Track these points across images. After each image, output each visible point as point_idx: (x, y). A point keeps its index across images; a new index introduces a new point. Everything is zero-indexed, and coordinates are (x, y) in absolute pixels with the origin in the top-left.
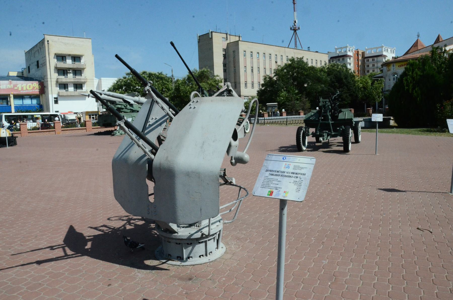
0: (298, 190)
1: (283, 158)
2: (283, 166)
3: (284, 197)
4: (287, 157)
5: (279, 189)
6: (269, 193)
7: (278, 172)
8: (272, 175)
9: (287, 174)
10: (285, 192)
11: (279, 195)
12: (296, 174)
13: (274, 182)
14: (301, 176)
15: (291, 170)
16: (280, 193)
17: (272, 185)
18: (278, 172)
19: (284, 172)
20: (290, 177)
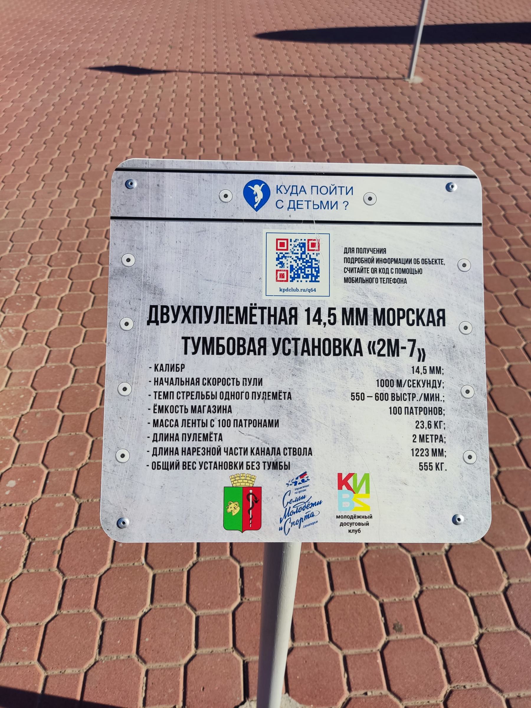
0: (430, 454)
1: (249, 195)
3: (353, 521)
4: (273, 182)
5: (299, 465)
6: (236, 509)
7: (244, 315)
8: (209, 346)
9: (316, 332)
10: (343, 482)
11: (301, 509)
12: (381, 317)
13: (241, 409)
14: (424, 334)
15: (333, 291)
16: (312, 492)
17: (232, 437)
18: (244, 315)
19: (288, 316)
20: (340, 348)
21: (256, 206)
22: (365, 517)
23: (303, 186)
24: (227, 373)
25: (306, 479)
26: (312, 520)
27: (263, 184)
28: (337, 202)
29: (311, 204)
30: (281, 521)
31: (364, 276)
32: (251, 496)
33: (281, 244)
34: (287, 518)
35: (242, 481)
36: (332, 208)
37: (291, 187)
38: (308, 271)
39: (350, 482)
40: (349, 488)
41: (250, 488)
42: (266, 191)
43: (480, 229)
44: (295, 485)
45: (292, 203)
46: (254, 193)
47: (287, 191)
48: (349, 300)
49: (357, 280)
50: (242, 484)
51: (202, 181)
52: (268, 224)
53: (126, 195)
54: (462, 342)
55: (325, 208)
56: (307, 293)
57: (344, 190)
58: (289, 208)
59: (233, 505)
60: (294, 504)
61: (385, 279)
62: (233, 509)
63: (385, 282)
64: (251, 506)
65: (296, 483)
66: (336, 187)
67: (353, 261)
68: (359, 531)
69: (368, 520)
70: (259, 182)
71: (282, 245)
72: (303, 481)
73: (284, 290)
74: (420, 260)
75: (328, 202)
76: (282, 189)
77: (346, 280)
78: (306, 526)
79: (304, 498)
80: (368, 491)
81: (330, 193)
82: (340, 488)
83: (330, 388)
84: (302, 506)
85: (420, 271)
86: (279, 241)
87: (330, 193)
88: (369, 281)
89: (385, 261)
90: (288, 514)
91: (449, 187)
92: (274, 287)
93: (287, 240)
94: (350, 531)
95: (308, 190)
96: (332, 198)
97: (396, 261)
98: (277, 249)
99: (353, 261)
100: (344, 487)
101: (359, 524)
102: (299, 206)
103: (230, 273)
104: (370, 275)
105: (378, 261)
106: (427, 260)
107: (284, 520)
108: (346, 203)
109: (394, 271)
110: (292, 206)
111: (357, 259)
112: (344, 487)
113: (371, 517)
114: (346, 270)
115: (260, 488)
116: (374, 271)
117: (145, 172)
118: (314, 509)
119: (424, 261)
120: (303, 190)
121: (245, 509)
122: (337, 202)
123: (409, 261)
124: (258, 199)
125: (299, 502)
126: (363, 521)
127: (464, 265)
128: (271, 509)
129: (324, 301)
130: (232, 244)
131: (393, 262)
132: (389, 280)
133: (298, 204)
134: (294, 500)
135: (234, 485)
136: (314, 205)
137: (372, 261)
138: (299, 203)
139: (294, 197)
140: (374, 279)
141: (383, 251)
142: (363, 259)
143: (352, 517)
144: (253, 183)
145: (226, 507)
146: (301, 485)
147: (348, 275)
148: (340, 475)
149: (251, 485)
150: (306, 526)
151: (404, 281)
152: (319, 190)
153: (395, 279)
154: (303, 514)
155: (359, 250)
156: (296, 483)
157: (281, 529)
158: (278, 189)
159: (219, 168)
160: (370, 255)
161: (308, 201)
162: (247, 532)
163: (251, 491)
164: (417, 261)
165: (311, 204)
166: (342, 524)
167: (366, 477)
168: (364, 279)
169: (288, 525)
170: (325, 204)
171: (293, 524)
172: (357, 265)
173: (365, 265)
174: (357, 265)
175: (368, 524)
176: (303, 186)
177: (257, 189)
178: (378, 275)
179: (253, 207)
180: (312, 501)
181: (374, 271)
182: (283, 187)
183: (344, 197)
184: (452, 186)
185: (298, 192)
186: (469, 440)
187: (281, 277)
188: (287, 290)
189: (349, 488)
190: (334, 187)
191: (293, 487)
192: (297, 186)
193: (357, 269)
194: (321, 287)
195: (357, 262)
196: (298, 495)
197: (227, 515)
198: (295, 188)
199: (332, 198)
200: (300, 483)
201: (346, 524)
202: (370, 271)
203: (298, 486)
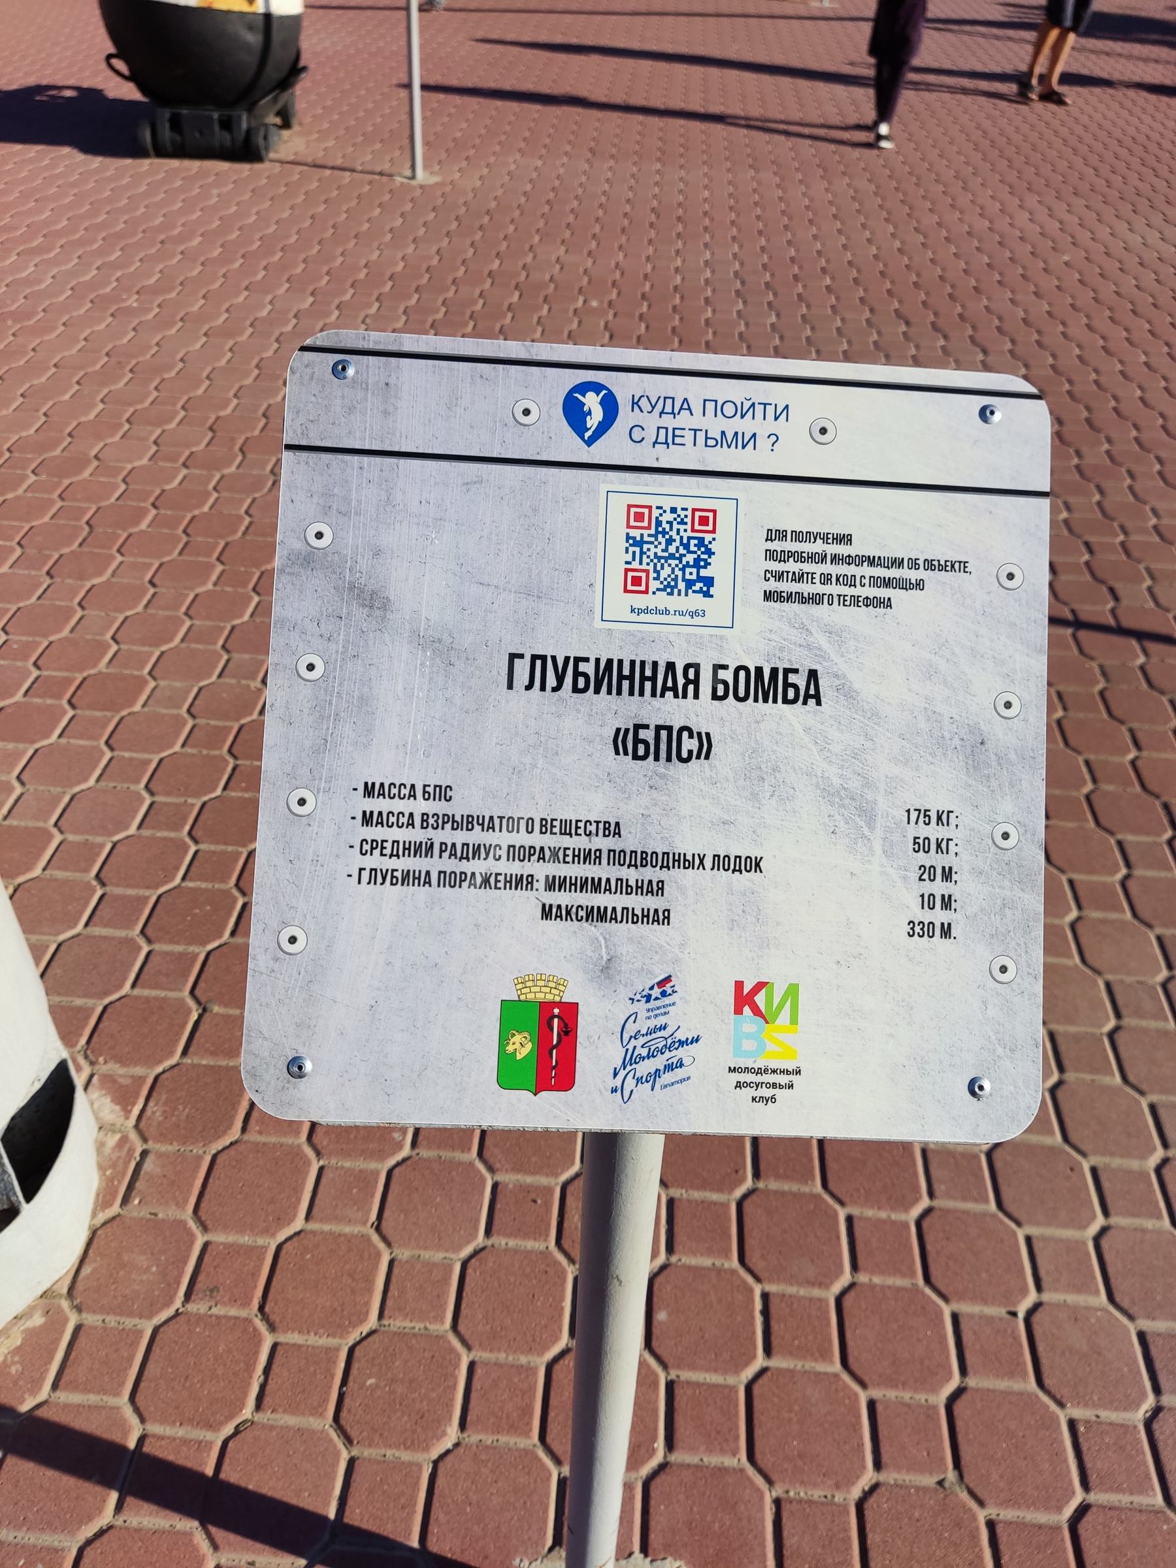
1: (574, 412)
2: (619, 557)
3: (763, 1081)
6: (523, 1047)
11: (656, 1054)
16: (682, 1017)
21: (587, 435)
22: (788, 1072)
23: (685, 399)
24: (514, 776)
25: (669, 991)
26: (679, 1073)
27: (604, 392)
28: (754, 435)
29: (701, 436)
30: (615, 1075)
31: (806, 588)
32: (556, 1020)
33: (637, 514)
34: (629, 1068)
35: (538, 989)
36: (744, 447)
37: (662, 400)
38: (691, 574)
39: (760, 999)
40: (757, 1011)
41: (554, 1004)
42: (610, 406)
43: (1046, 503)
44: (648, 1001)
45: (662, 432)
46: (586, 408)
47: (653, 408)
48: (773, 636)
49: (790, 597)
50: (538, 995)
51: (479, 380)
52: (611, 475)
53: (320, 400)
54: (999, 733)
55: (729, 447)
56: (687, 620)
57: (770, 410)
58: (655, 443)
59: (518, 1038)
60: (642, 1040)
61: (848, 598)
62: (518, 1046)
63: (847, 603)
64: (555, 1042)
65: (648, 998)
66: (753, 404)
67: (785, 556)
68: (773, 1099)
69: (791, 1077)
70: (596, 387)
71: (639, 517)
72: (664, 994)
73: (640, 612)
74: (921, 562)
75: (736, 434)
76: (644, 403)
77: (768, 596)
78: (666, 1086)
79: (665, 1028)
80: (794, 1020)
81: (742, 416)
82: (738, 1011)
83: (727, 818)
84: (660, 1045)
85: (919, 585)
86: (633, 510)
87: (742, 416)
88: (816, 599)
89: (849, 560)
90: (631, 1060)
91: (985, 414)
92: (619, 603)
93: (650, 508)
94: (754, 1099)
95: (697, 408)
96: (746, 426)
97: (872, 561)
98: (628, 526)
99: (785, 556)
100: (747, 1010)
101: (774, 1085)
102: (677, 440)
103: (530, 570)
104: (818, 588)
105: (836, 559)
106: (936, 563)
107: (622, 1073)
108: (773, 438)
109: (866, 581)
110: (662, 439)
111: (791, 554)
112: (747, 1010)
113: (798, 1072)
114: (768, 575)
115: (575, 1006)
116: (826, 579)
117: (360, 357)
118: (681, 1053)
119: (930, 565)
120: (685, 406)
121: (543, 1047)
122: (754, 435)
123: (898, 563)
124: (593, 422)
125: (654, 1036)
126: (783, 1079)
127: (1011, 576)
128: (596, 1053)
129: (722, 638)
130: (535, 510)
131: (865, 564)
132: (855, 601)
133: (674, 436)
134: (644, 1031)
135: (523, 997)
136: (707, 438)
137: (823, 559)
138: (677, 432)
139: (667, 421)
140: (826, 597)
141: (845, 539)
142: (805, 555)
143: (759, 1072)
144: (584, 388)
145: (503, 1041)
146: (658, 1003)
147: (773, 585)
148: (739, 985)
149: (557, 999)
150: (666, 1086)
151: (887, 603)
152: (719, 409)
153: (867, 598)
154: (659, 1062)
155: (798, 536)
156: (648, 998)
157: (614, 1090)
158: (635, 403)
159: (513, 355)
160: (818, 547)
161: (695, 430)
162: (543, 1093)
163: (556, 1011)
164: (914, 564)
165: (701, 436)
166: (739, 1085)
167: (793, 991)
168: (806, 595)
169: (630, 1083)
170: (730, 437)
171: (639, 1081)
172: (792, 566)
173: (807, 567)
174: (792, 566)
175: (791, 1086)
176: (685, 399)
177: (592, 401)
178: (834, 589)
179: (582, 438)
180: (681, 1035)
181: (826, 579)
182: (644, 400)
183: (770, 426)
184: (992, 413)
185: (676, 411)
186: (1003, 935)
187: (634, 583)
188: (647, 611)
189: (757, 1011)
190: (750, 403)
191: (641, 1007)
192: (673, 399)
193: (790, 575)
194: (716, 607)
195: (791, 559)
196: (652, 1023)
197: (505, 1058)
198: (669, 402)
199: (746, 426)
200: (657, 999)
201: (748, 1085)
202: (817, 580)
203: (652, 1004)
